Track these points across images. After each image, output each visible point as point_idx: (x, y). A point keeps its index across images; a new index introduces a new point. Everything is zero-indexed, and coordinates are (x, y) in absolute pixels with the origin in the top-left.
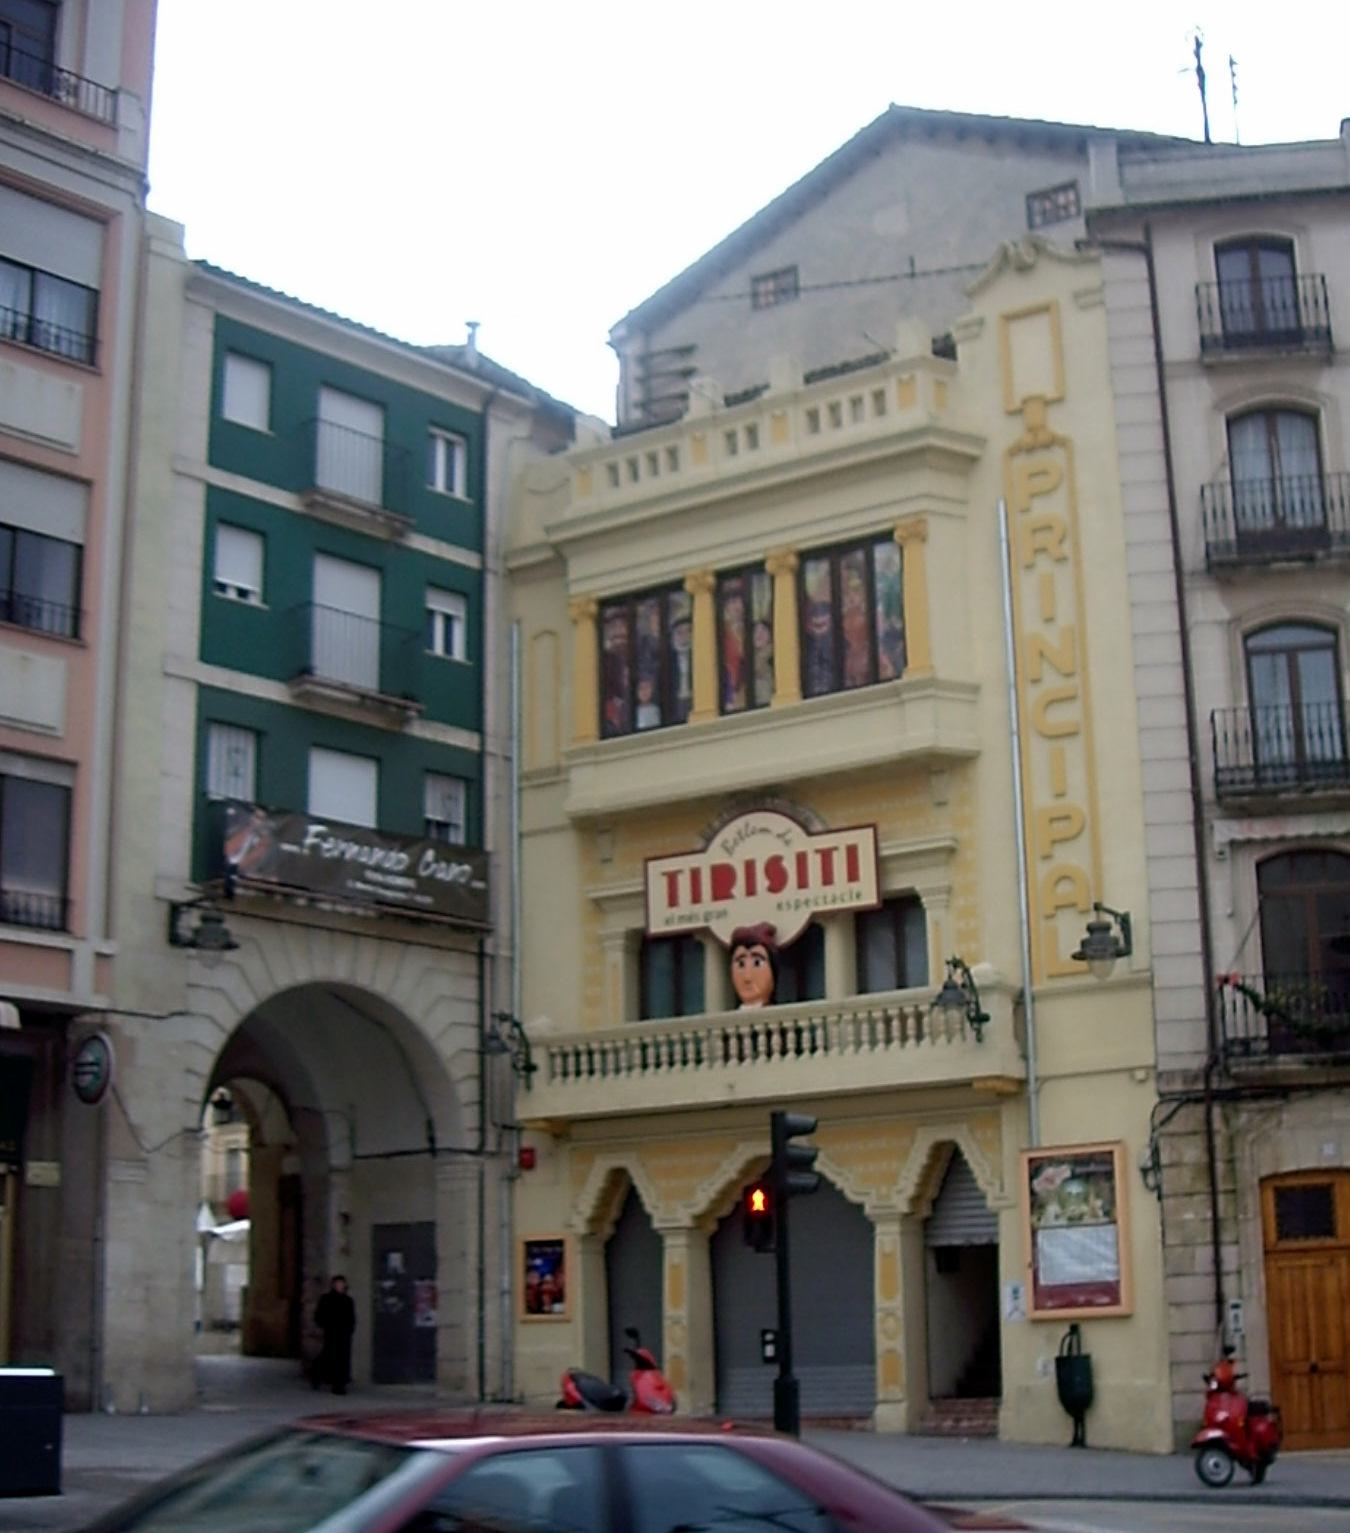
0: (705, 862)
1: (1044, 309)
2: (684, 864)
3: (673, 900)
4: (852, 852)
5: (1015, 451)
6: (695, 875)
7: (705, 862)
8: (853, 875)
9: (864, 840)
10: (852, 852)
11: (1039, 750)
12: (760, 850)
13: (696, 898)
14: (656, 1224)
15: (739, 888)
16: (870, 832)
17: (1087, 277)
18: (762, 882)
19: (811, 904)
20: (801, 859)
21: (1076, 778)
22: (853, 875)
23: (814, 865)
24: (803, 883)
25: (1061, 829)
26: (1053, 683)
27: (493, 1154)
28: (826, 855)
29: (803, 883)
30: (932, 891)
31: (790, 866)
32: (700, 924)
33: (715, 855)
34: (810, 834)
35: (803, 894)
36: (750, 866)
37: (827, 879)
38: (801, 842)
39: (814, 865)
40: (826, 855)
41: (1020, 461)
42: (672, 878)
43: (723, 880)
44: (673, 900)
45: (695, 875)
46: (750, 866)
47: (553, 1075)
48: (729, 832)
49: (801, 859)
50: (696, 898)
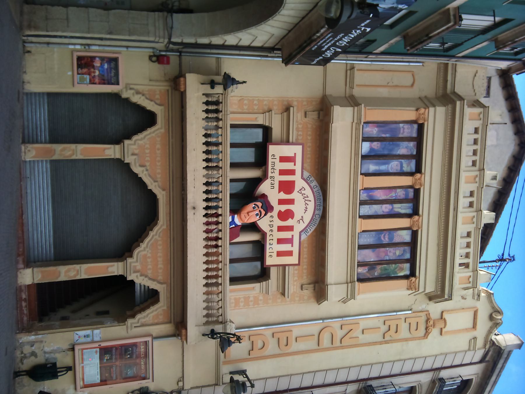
1: (474, 326)
2: (298, 168)
3: (283, 159)
4: (289, 253)
6: (292, 172)
7: (297, 178)
8: (280, 254)
9: (293, 259)
10: (289, 253)
12: (297, 208)
13: (283, 172)
14: (127, 142)
15: (283, 196)
16: (297, 263)
17: (480, 343)
18: (284, 208)
19: (271, 233)
21: (302, 346)
22: (280, 254)
24: (281, 229)
25: (283, 342)
28: (289, 241)
29: (281, 229)
31: (289, 222)
32: (270, 174)
33: (300, 183)
34: (300, 233)
35: (275, 229)
37: (280, 241)
38: (299, 227)
40: (289, 241)
41: (424, 318)
44: (283, 159)
45: (292, 172)
47: (207, 95)
48: (308, 192)
49: (290, 228)
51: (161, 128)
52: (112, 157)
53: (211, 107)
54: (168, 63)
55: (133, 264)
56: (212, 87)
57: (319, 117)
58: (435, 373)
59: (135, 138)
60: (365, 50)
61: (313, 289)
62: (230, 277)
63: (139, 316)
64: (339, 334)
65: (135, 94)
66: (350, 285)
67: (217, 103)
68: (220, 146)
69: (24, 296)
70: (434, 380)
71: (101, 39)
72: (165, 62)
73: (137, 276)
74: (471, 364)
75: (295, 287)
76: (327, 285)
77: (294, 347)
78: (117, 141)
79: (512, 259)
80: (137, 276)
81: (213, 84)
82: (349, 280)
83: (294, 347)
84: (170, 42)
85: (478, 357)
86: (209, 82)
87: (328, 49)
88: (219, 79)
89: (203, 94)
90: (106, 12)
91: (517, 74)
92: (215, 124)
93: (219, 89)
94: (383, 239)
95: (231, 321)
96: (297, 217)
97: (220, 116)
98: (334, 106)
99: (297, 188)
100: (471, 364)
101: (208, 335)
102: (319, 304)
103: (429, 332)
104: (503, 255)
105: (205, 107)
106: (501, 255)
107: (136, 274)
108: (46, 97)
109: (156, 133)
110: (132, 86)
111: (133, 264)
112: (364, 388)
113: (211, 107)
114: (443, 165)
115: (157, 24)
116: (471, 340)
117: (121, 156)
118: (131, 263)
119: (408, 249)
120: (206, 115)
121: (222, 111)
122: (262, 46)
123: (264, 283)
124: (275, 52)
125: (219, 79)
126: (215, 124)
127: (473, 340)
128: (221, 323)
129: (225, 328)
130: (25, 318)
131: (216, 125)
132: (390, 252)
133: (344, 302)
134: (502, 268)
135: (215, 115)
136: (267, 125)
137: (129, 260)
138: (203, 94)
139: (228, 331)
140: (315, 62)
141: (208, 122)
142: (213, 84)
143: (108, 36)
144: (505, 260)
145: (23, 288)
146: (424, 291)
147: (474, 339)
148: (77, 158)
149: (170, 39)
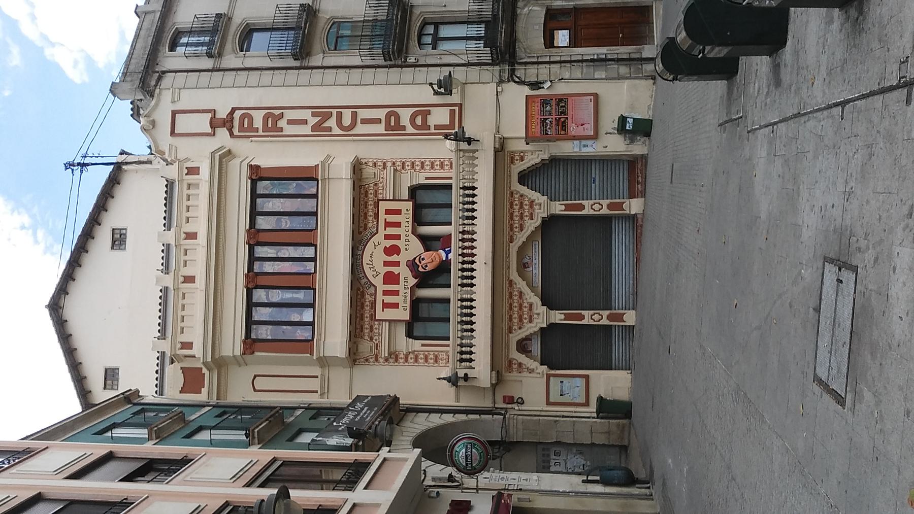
0: (381, 287)
2: (380, 297)
3: (396, 306)
4: (388, 212)
5: (232, 135)
6: (386, 293)
7: (381, 287)
8: (398, 212)
9: (383, 206)
10: (388, 212)
11: (360, 129)
12: (380, 257)
13: (396, 293)
14: (545, 325)
15: (395, 270)
18: (394, 258)
19: (407, 233)
20: (387, 237)
22: (398, 212)
23: (392, 231)
24: (398, 237)
26: (332, 123)
28: (388, 224)
29: (398, 237)
30: (411, 178)
32: (409, 291)
33: (378, 282)
35: (403, 238)
36: (386, 264)
37: (398, 225)
38: (379, 238)
39: (392, 231)
40: (388, 224)
42: (386, 306)
43: (391, 278)
44: (396, 306)
45: (386, 293)
46: (386, 264)
48: (369, 273)
49: (387, 237)
50: (396, 293)
51: (512, 337)
52: (557, 312)
54: (504, 397)
55: (542, 211)
56: (466, 375)
57: (357, 346)
58: (218, 66)
60: (315, 411)
61: (363, 173)
63: (538, 161)
64: (332, 123)
66: (326, 177)
67: (462, 360)
68: (459, 321)
69: (639, 186)
70: (219, 56)
71: (563, 417)
74: (176, 72)
75: (381, 176)
76: (351, 178)
77: (381, 114)
78: (552, 326)
79: (69, 165)
80: (538, 200)
81: (466, 378)
82: (327, 181)
83: (381, 114)
84: (504, 415)
85: (168, 80)
86: (469, 379)
87: (362, 409)
88: (461, 383)
89: (474, 368)
90: (558, 440)
91: (131, 390)
92: (464, 341)
93: (461, 374)
94: (288, 222)
95: (452, 151)
96: (381, 249)
97: (459, 349)
98: (345, 357)
99: (381, 277)
100: (176, 72)
101: (474, 140)
102: (356, 156)
104: (82, 171)
106: (84, 171)
107: (539, 202)
108: (613, 367)
109: (517, 333)
110: (539, 376)
112: (303, 59)
114: (222, 295)
115: (515, 430)
116: (178, 101)
117: (549, 312)
119: (259, 209)
120: (472, 349)
122: (417, 413)
123: (415, 184)
124: (405, 408)
125: (461, 383)
126: (464, 341)
127: (176, 100)
128: (460, 150)
129: (457, 145)
130: (639, 166)
131: (463, 340)
132: (279, 207)
133: (328, 156)
134: (80, 155)
136: (411, 340)
137: (545, 215)
138: (474, 368)
139: (455, 142)
140: (369, 398)
141: (471, 343)
142: (466, 378)
143: (558, 419)
144: (79, 164)
145: (640, 195)
146: (241, 162)
147: (175, 102)
148: (588, 311)
149: (504, 418)
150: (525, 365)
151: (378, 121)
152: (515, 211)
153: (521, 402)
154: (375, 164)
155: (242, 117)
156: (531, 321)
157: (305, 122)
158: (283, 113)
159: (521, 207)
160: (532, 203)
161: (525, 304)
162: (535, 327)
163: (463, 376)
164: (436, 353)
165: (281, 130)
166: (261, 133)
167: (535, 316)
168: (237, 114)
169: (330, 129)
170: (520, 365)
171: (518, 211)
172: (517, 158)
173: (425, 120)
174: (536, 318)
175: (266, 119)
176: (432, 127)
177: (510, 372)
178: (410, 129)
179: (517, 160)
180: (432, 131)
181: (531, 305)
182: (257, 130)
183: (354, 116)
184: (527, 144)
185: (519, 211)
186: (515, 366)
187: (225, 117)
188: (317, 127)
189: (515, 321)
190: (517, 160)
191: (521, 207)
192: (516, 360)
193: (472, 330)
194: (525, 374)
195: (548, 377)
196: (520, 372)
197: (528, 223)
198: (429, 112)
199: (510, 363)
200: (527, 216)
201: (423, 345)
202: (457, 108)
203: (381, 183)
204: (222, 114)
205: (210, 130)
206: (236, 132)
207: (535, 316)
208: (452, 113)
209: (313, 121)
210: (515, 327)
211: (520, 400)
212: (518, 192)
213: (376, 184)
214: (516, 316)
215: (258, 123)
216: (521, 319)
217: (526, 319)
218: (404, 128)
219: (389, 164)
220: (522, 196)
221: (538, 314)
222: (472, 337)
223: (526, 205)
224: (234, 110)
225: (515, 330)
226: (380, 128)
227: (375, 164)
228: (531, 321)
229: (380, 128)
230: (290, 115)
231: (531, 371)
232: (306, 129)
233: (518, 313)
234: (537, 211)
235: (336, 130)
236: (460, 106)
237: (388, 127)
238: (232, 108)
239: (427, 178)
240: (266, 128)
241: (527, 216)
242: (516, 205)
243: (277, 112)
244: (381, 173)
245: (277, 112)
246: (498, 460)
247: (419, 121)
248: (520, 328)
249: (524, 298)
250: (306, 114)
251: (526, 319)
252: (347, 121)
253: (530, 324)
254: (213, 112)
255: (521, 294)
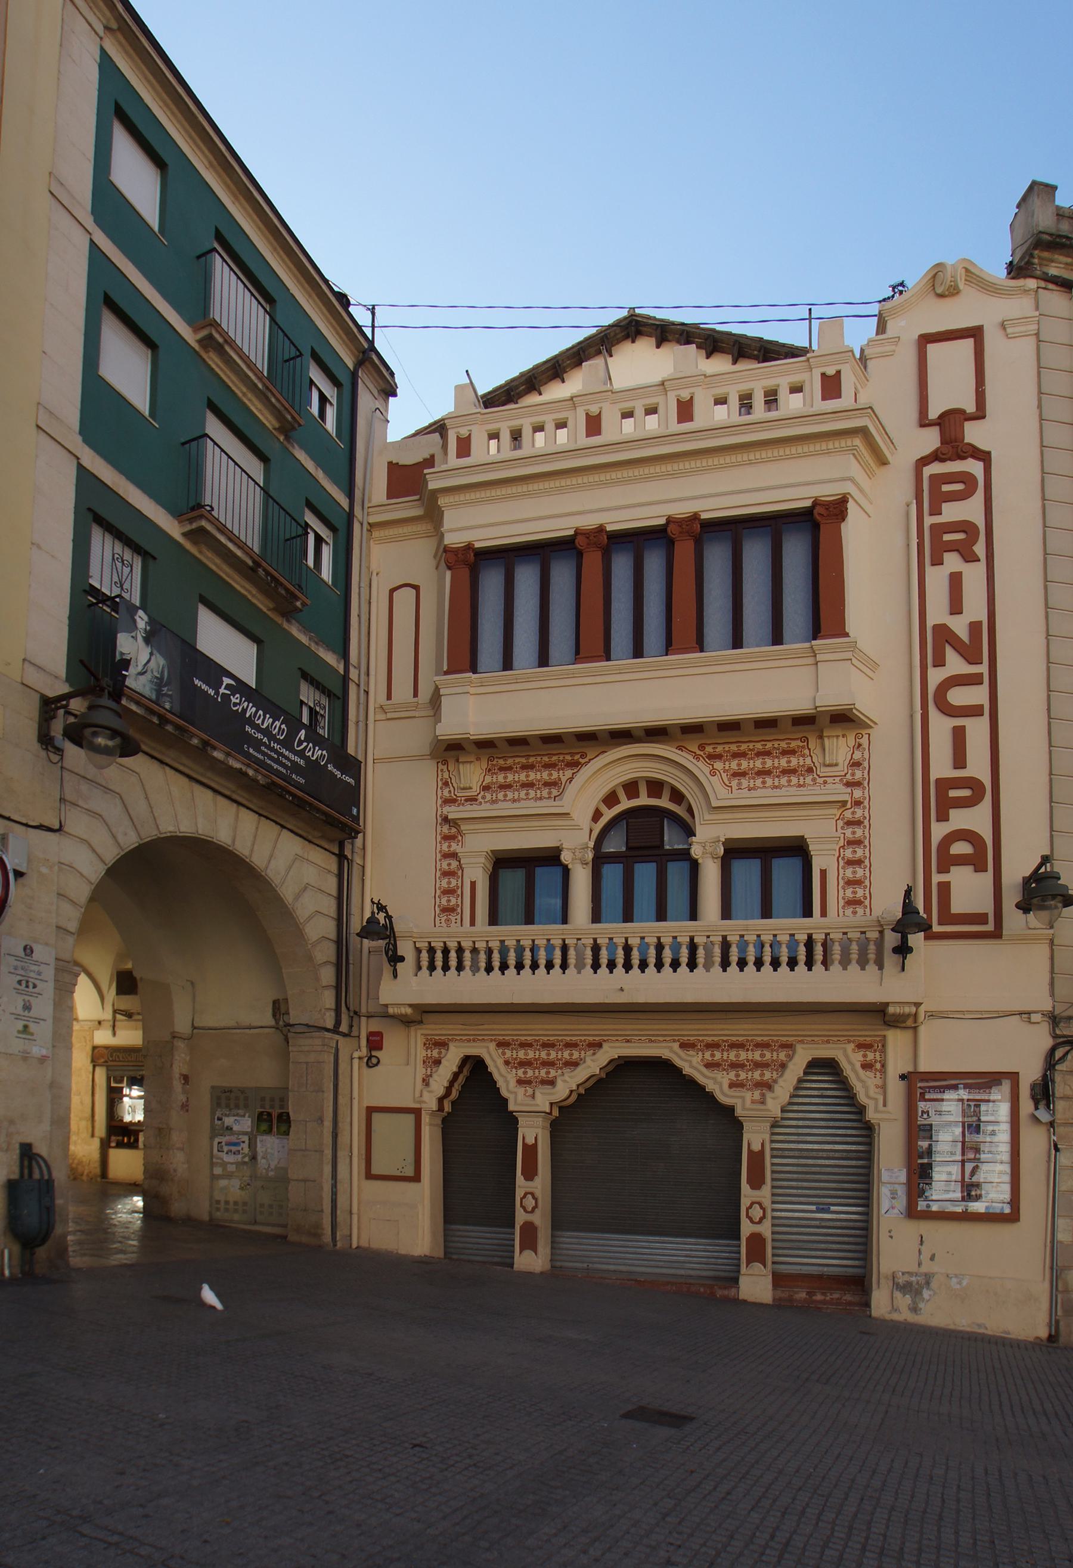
26: (956, 664)
27: (345, 1035)
53: (439, 963)
54: (380, 1034)
56: (402, 959)
59: (504, 1093)
62: (802, 916)
64: (956, 664)
65: (429, 1089)
72: (378, 1038)
73: (774, 1098)
77: (978, 767)
83: (978, 767)
84: (335, 1030)
102: (876, 723)
103: (973, 452)
105: (439, 971)
111: (748, 1104)
113: (439, 963)
115: (306, 1048)
118: (744, 1109)
121: (445, 943)
133: (874, 666)
135: (453, 955)
149: (328, 1030)
150: (437, 1071)
151: (959, 759)
152: (750, 1052)
153: (371, 1062)
154: (857, 764)
155: (967, 479)
156: (520, 1082)
157: (956, 607)
158: (979, 560)
159: (758, 1065)
160: (768, 1086)
161: (553, 1073)
162: (508, 1090)
163: (399, 953)
164: (459, 910)
165: (937, 562)
166: (929, 521)
167: (530, 1091)
168: (975, 467)
169: (940, 662)
170: (438, 1062)
171: (750, 1058)
172: (870, 1056)
173: (961, 860)
174: (526, 1091)
175: (966, 527)
176: (943, 878)
177: (425, 1044)
178: (938, 831)
179: (865, 1056)
180: (936, 878)
181: (552, 1083)
182: (936, 511)
183: (974, 711)
184: (903, 1077)
185: (748, 1060)
186: (435, 1053)
187: (966, 441)
188: (944, 635)
189: (521, 1054)
190: (865, 1056)
191: (758, 1065)
192: (446, 1055)
193: (489, 969)
194: (421, 1072)
195: (417, 1113)
196: (424, 1062)
197: (723, 1078)
198: (980, 868)
199: (442, 1045)
200: (737, 1076)
201: (473, 884)
202: (990, 927)
203: (814, 780)
204: (974, 434)
205: (933, 414)
206: (936, 468)
207: (530, 1091)
208: (981, 919)
209: (959, 626)
210: (508, 1053)
211: (374, 1061)
212: (790, 1057)
213: (810, 770)
214: (531, 1054)
215: (952, 512)
216: (524, 1064)
217: (525, 1073)
218: (943, 817)
219: (858, 793)
220: (783, 1066)
221: (533, 1096)
222: (475, 969)
223: (762, 1075)
224: (984, 457)
225: (504, 1054)
226: (942, 767)
227: (857, 764)
228: (520, 1082)
229: (942, 767)
230: (974, 576)
231: (426, 1082)
232: (938, 613)
233: (536, 1060)
234: (748, 1095)
235: (936, 676)
236: (996, 934)
237: (944, 784)
238: (989, 453)
239: (823, 873)
240: (938, 530)
241: (737, 1076)
242: (763, 1056)
243: (980, 549)
244: (837, 779)
245: (980, 549)
246: (272, 1023)
247: (961, 848)
248: (507, 1063)
249: (566, 1070)
250: (975, 608)
251: (525, 1073)
252: (958, 697)
253: (515, 1080)
254: (980, 414)
255: (575, 1064)
